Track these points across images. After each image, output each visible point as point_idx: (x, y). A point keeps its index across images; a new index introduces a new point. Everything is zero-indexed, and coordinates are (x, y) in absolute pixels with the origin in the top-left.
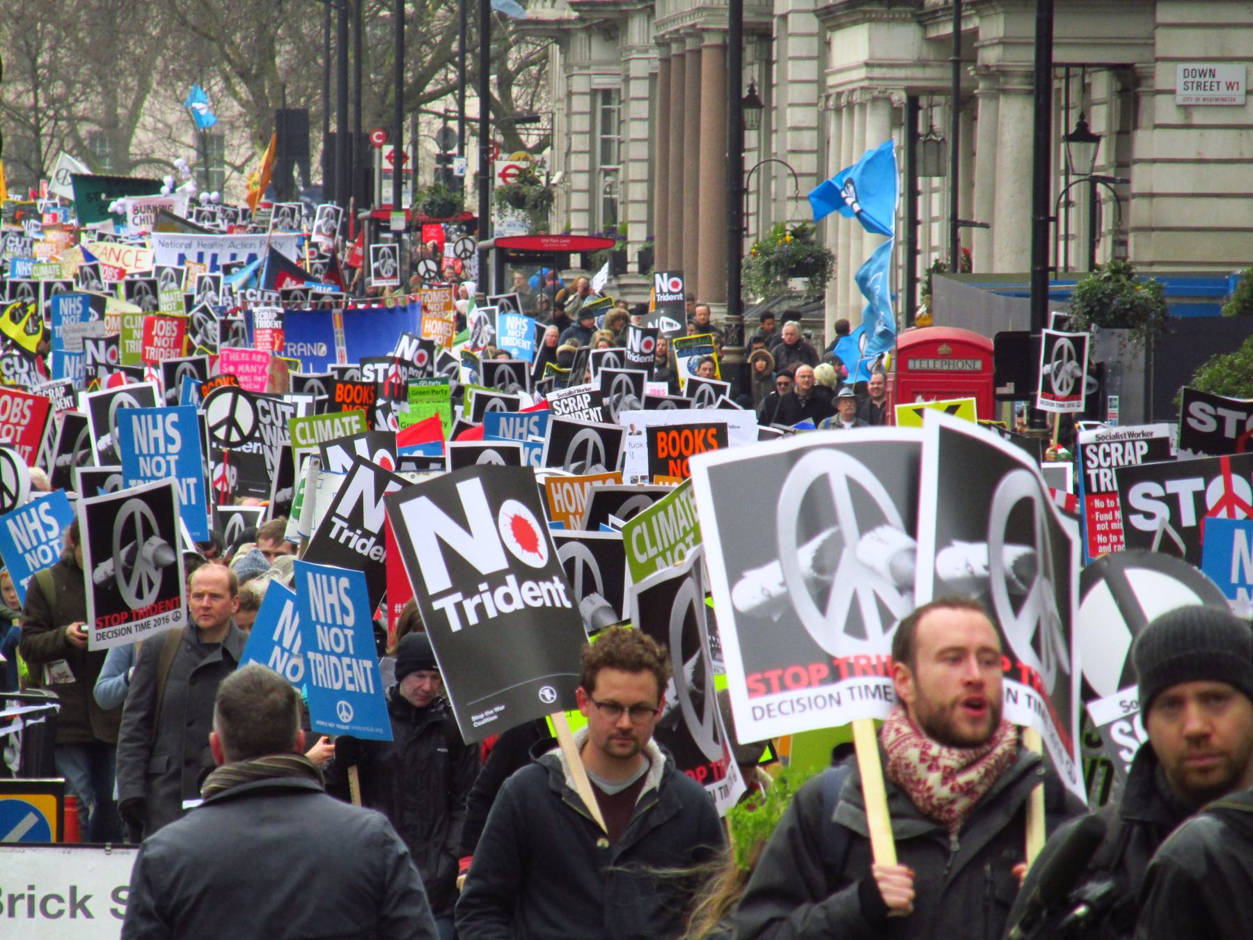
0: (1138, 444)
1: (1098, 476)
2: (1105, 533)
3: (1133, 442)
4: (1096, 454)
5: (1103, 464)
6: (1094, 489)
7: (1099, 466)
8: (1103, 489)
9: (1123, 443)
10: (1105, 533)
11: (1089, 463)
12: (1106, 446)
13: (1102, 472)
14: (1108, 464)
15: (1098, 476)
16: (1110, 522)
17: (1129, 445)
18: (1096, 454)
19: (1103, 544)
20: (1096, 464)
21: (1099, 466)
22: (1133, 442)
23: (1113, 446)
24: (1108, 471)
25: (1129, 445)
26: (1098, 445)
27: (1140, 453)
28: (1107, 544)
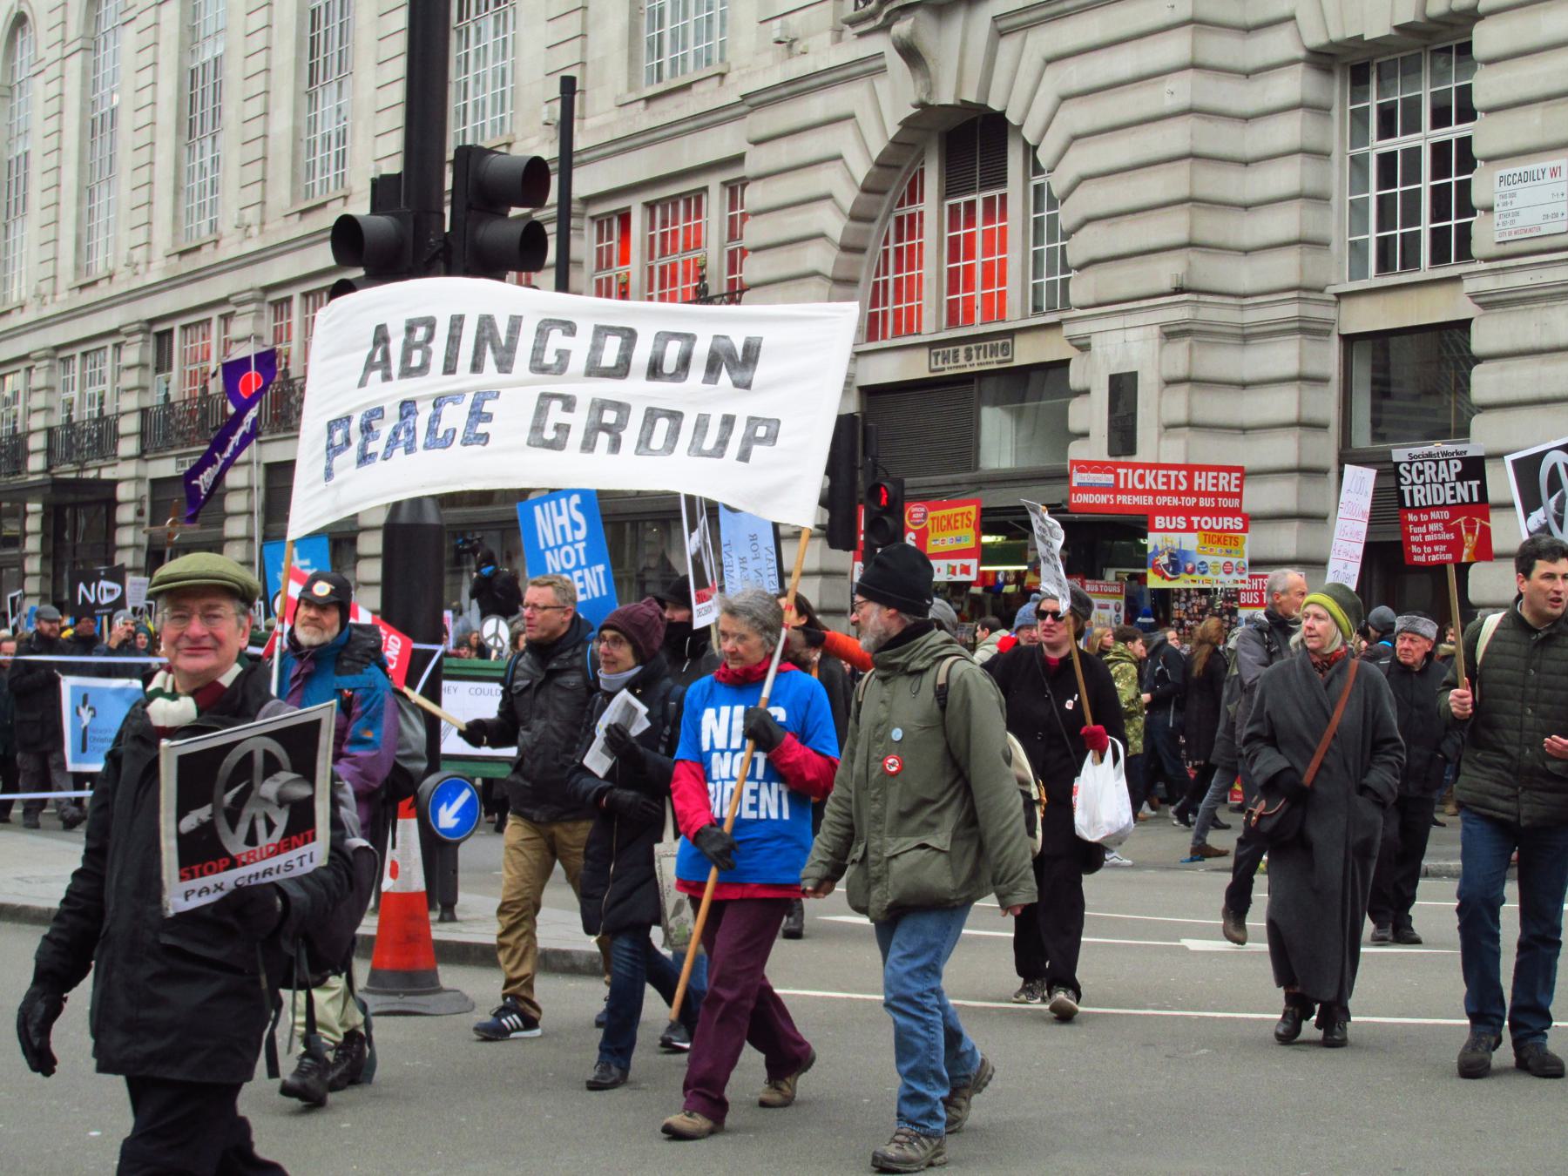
0: (1452, 463)
1: (1411, 492)
2: (1419, 544)
3: (1447, 461)
4: (1410, 472)
5: (1416, 481)
6: (1408, 504)
7: (1413, 484)
8: (1417, 504)
9: (1437, 462)
10: (1419, 544)
11: (1402, 480)
12: (1420, 465)
13: (1415, 488)
14: (1421, 481)
15: (1411, 492)
16: (1423, 535)
17: (1442, 464)
18: (1410, 472)
19: (1417, 554)
20: (1409, 481)
21: (1413, 484)
22: (1447, 461)
23: (1426, 464)
24: (1422, 488)
25: (1442, 464)
26: (1411, 464)
27: (1453, 471)
28: (1421, 554)
